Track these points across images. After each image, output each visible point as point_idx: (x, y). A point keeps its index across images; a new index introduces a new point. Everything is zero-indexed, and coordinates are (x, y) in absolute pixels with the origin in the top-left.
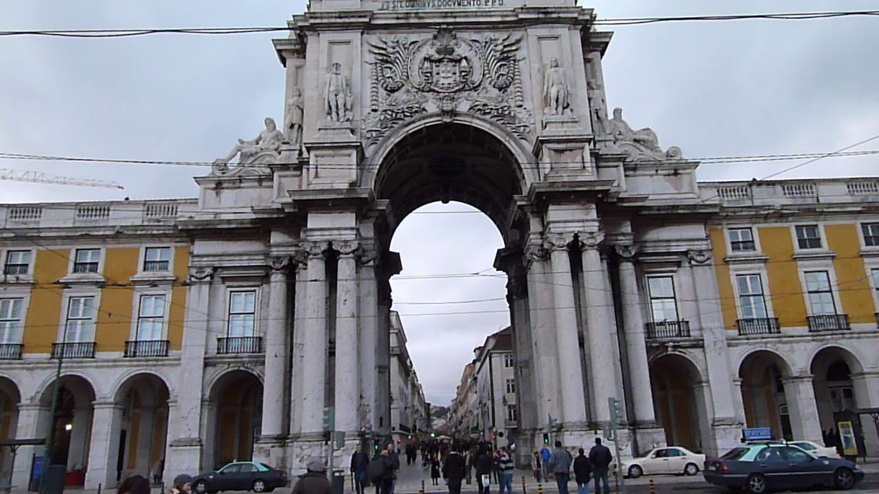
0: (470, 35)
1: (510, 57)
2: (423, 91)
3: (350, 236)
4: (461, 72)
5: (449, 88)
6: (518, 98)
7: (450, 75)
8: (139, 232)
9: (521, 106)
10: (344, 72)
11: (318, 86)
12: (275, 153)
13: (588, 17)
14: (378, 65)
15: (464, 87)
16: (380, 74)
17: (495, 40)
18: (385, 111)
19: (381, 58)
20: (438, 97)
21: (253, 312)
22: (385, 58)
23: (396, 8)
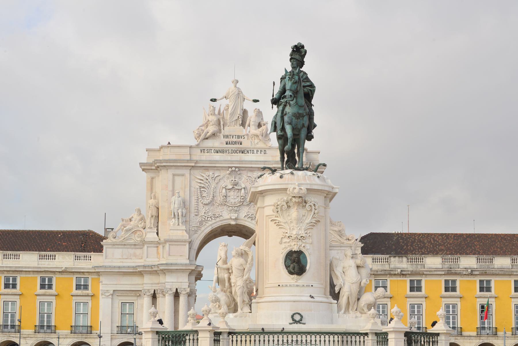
0: (247, 173)
2: (221, 205)
3: (185, 285)
4: (241, 196)
7: (236, 197)
8: (73, 270)
10: (182, 194)
11: (167, 200)
12: (142, 230)
14: (198, 189)
15: (243, 204)
19: (200, 185)
20: (229, 209)
21: (133, 313)
22: (202, 185)
23: (208, 153)
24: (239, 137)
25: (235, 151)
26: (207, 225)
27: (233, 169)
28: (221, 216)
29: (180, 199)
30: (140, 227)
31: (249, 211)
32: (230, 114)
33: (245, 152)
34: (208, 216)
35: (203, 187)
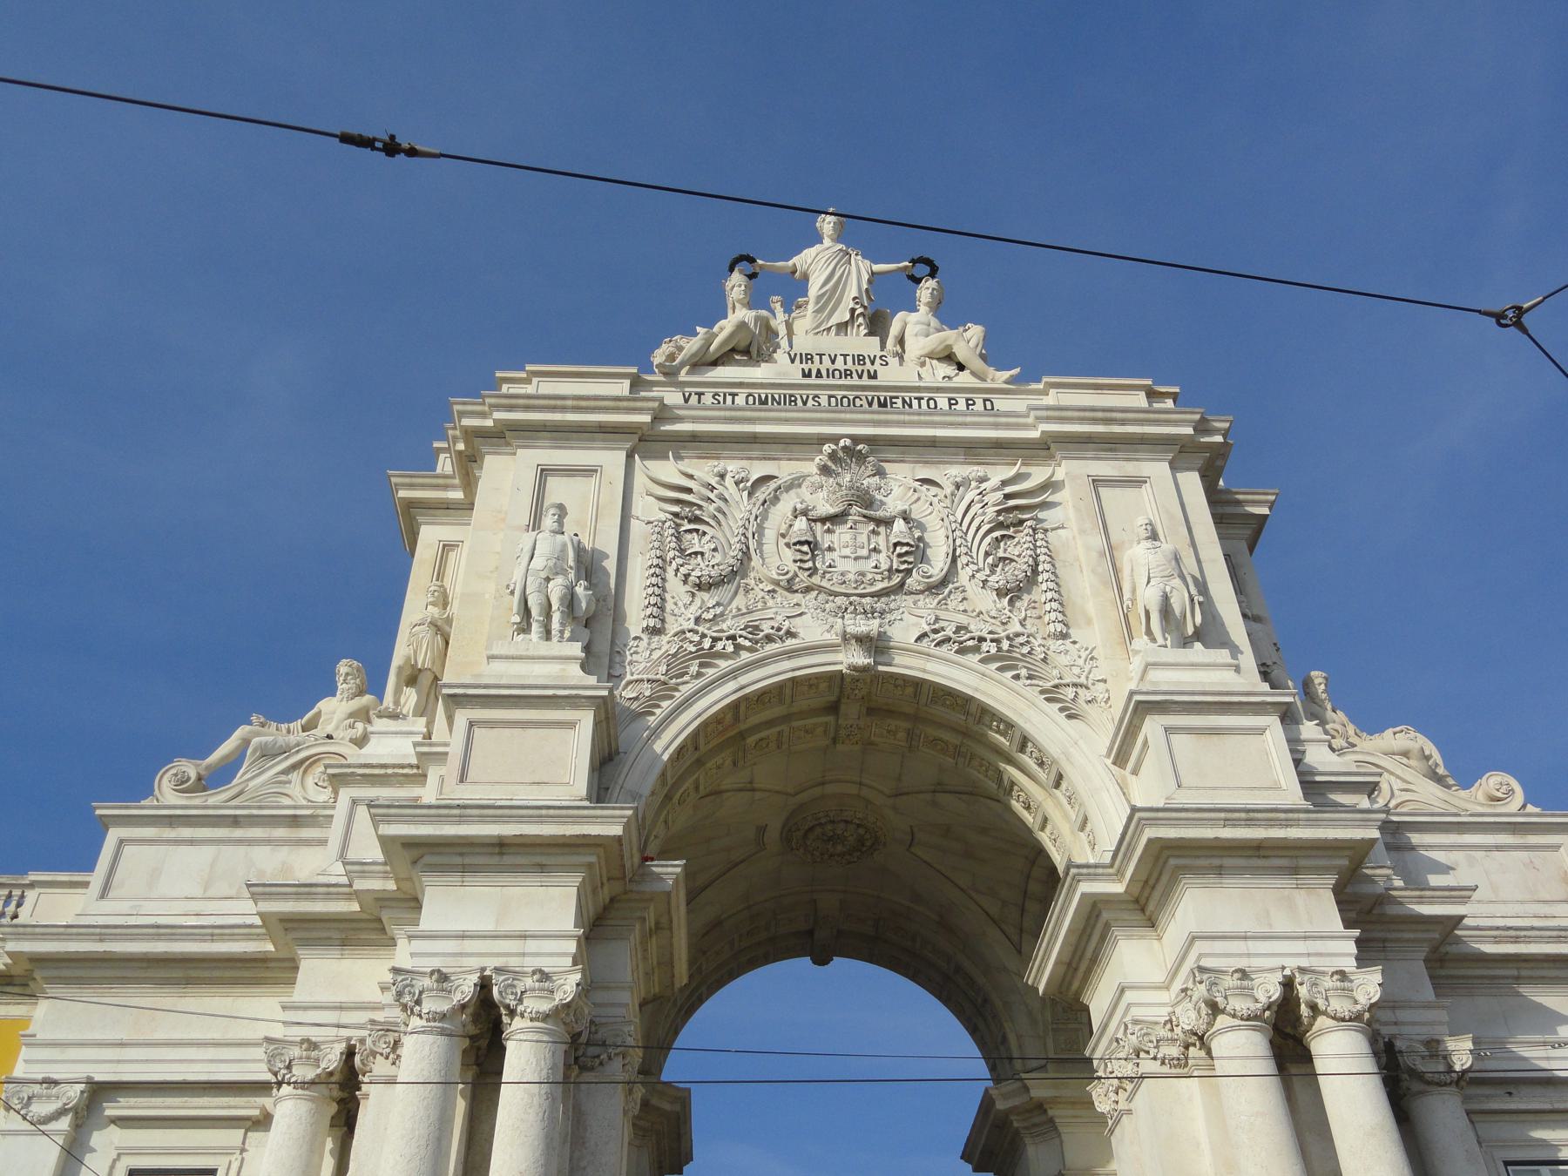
1: (1021, 522)
4: (895, 545)
5: (859, 583)
6: (1053, 616)
7: (865, 552)
9: (1064, 636)
11: (497, 568)
13: (1219, 439)
14: (667, 524)
15: (902, 584)
16: (673, 545)
17: (982, 480)
18: (683, 632)
19: (676, 509)
24: (860, 359)
25: (845, 400)
26: (710, 671)
27: (842, 443)
28: (791, 634)
29: (566, 538)
30: (342, 739)
31: (942, 614)
32: (819, 298)
33: (892, 403)
34: (715, 634)
35: (697, 520)
